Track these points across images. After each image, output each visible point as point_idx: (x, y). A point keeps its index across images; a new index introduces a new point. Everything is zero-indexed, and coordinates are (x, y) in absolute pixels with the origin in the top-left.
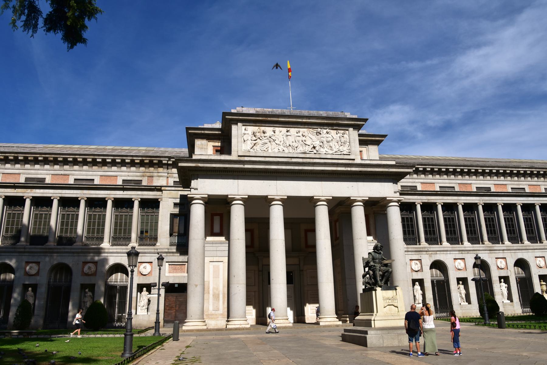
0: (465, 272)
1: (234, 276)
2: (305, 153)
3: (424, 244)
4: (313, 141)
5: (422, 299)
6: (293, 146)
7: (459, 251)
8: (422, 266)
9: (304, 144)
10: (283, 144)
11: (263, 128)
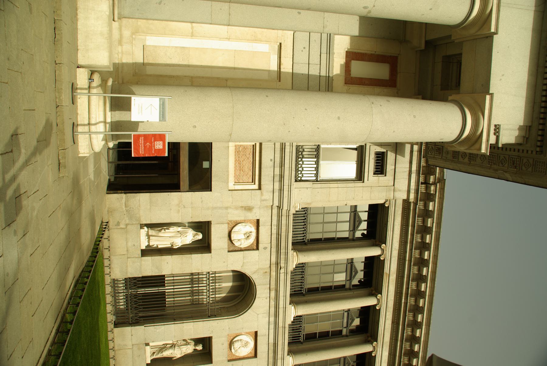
0: (225, 359)
5: (160, 247)
7: (275, 345)
8: (241, 250)
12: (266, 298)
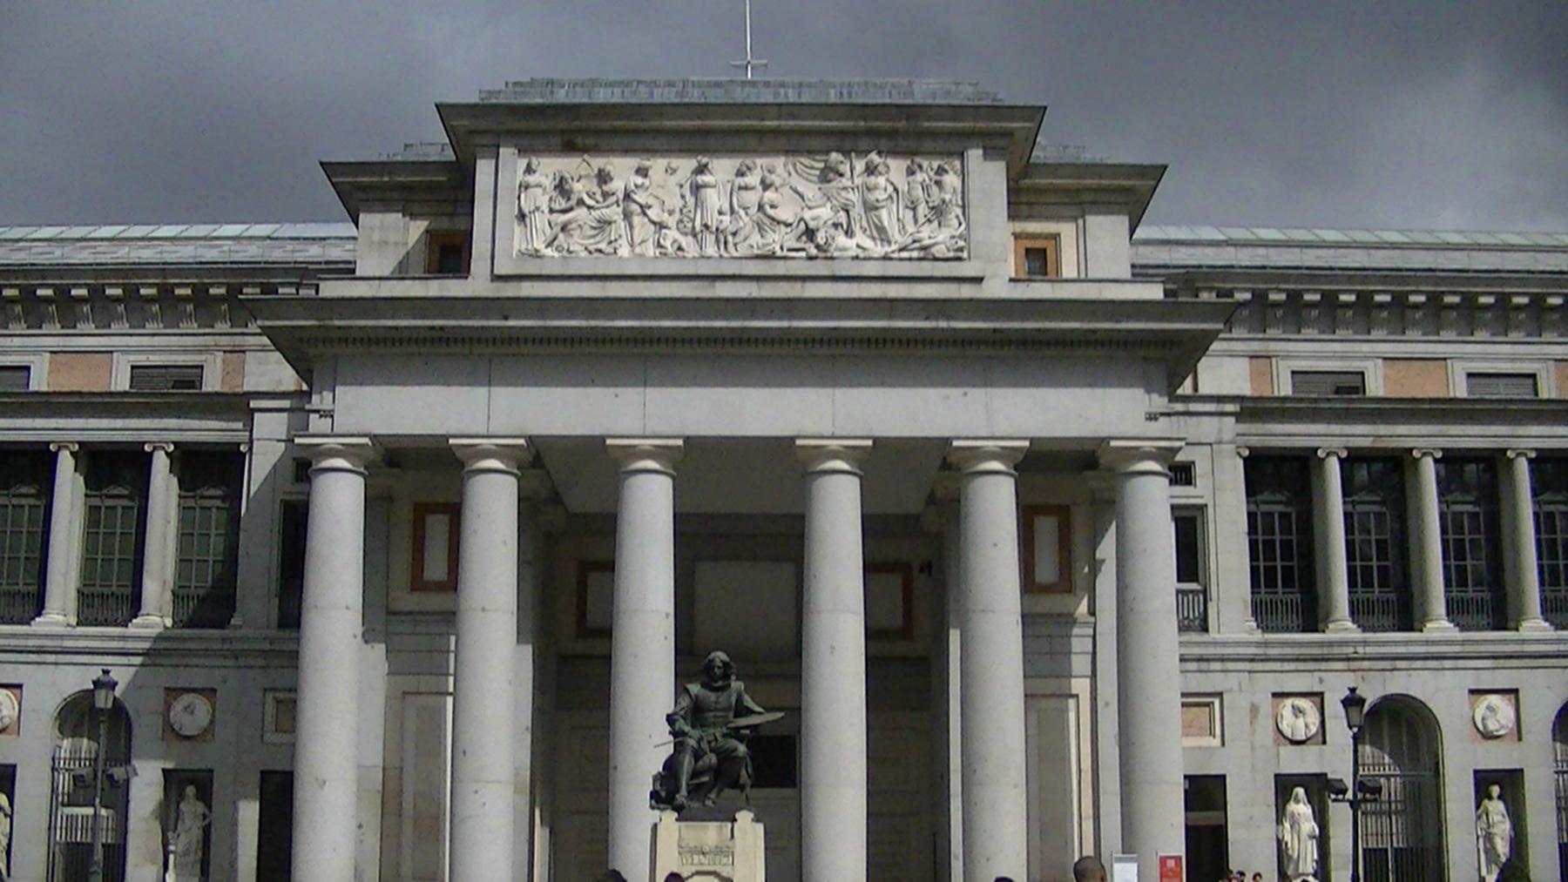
1: (464, 752)
2: (772, 257)
3: (1343, 627)
4: (809, 204)
5: (1316, 857)
6: (721, 227)
8: (1323, 722)
9: (766, 221)
10: (681, 221)
11: (598, 162)
12: (1410, 675)
